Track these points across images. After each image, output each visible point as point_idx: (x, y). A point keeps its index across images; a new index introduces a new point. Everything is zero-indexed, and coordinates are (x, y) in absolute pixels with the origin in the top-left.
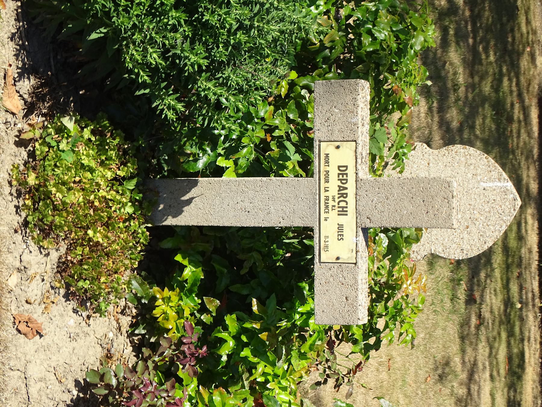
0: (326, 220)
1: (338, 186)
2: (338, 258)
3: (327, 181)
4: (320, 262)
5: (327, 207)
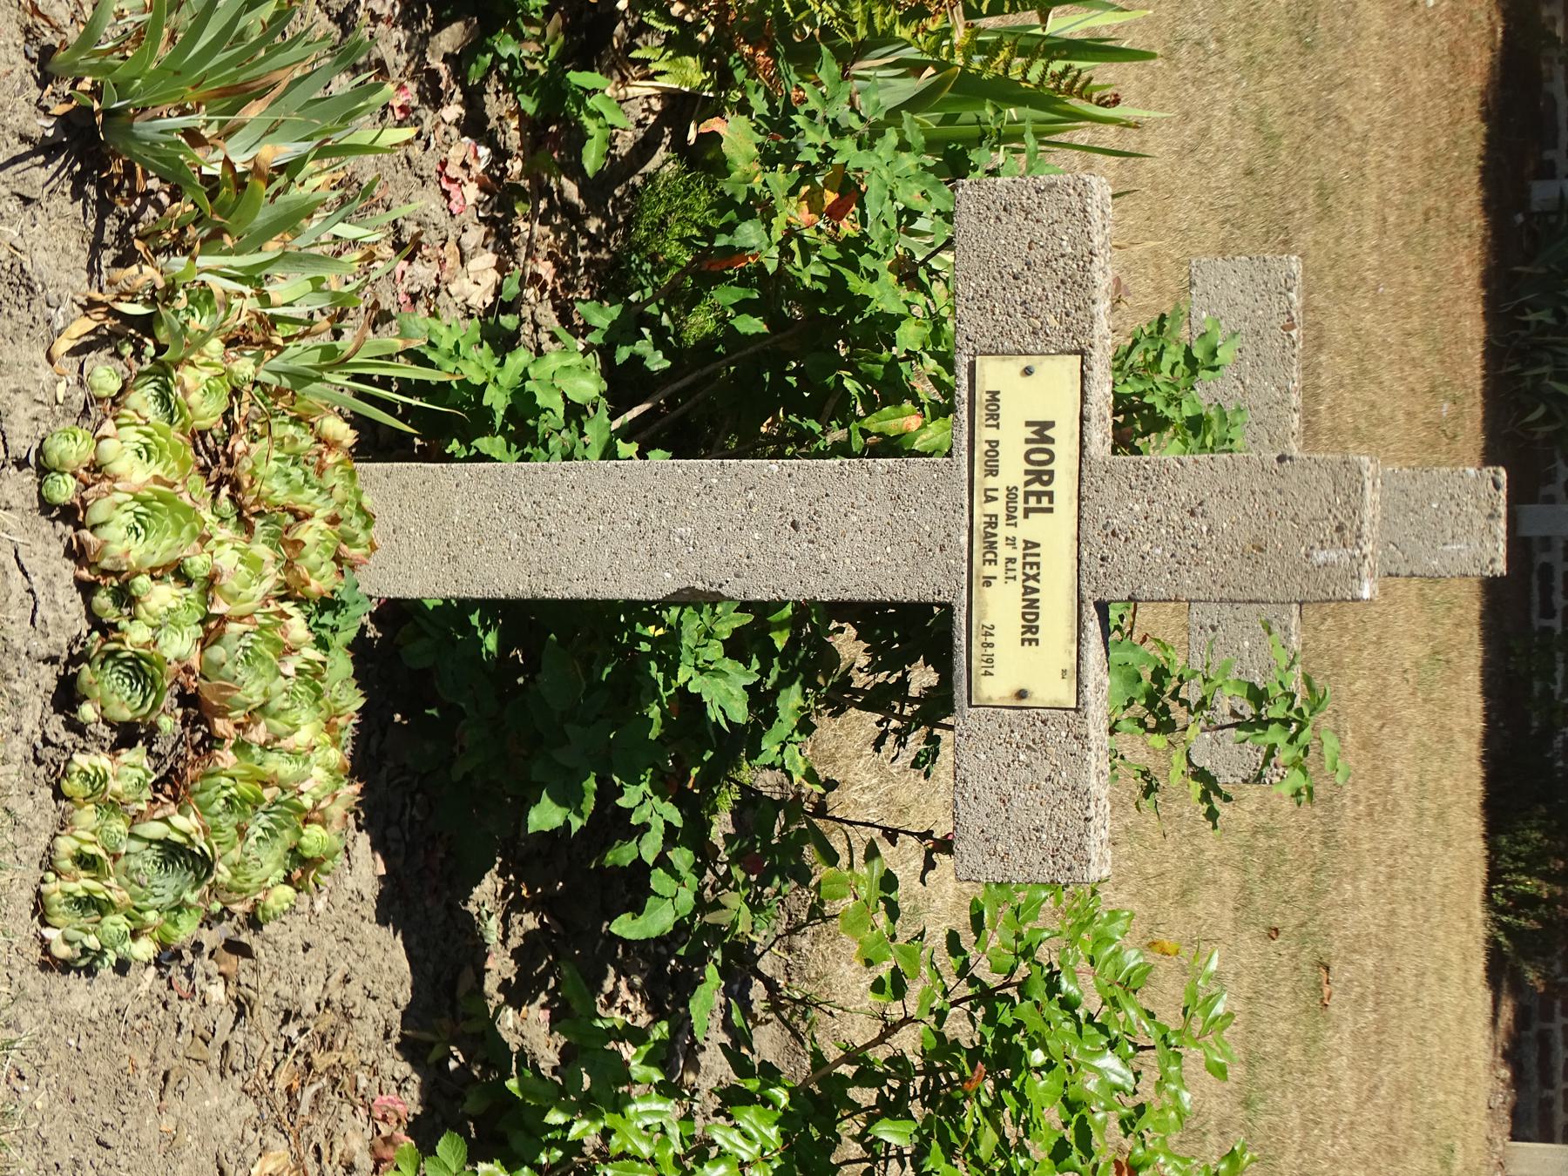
0: (988, 584)
2: (1022, 694)
3: (993, 472)
4: (970, 706)
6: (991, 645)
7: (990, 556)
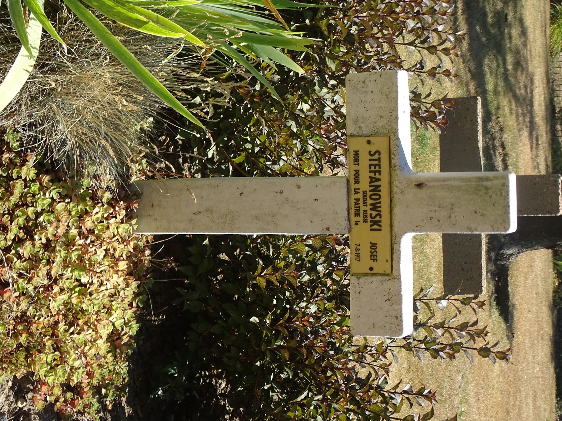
1: (370, 177)
2: (371, 269)
3: (357, 182)
6: (359, 250)
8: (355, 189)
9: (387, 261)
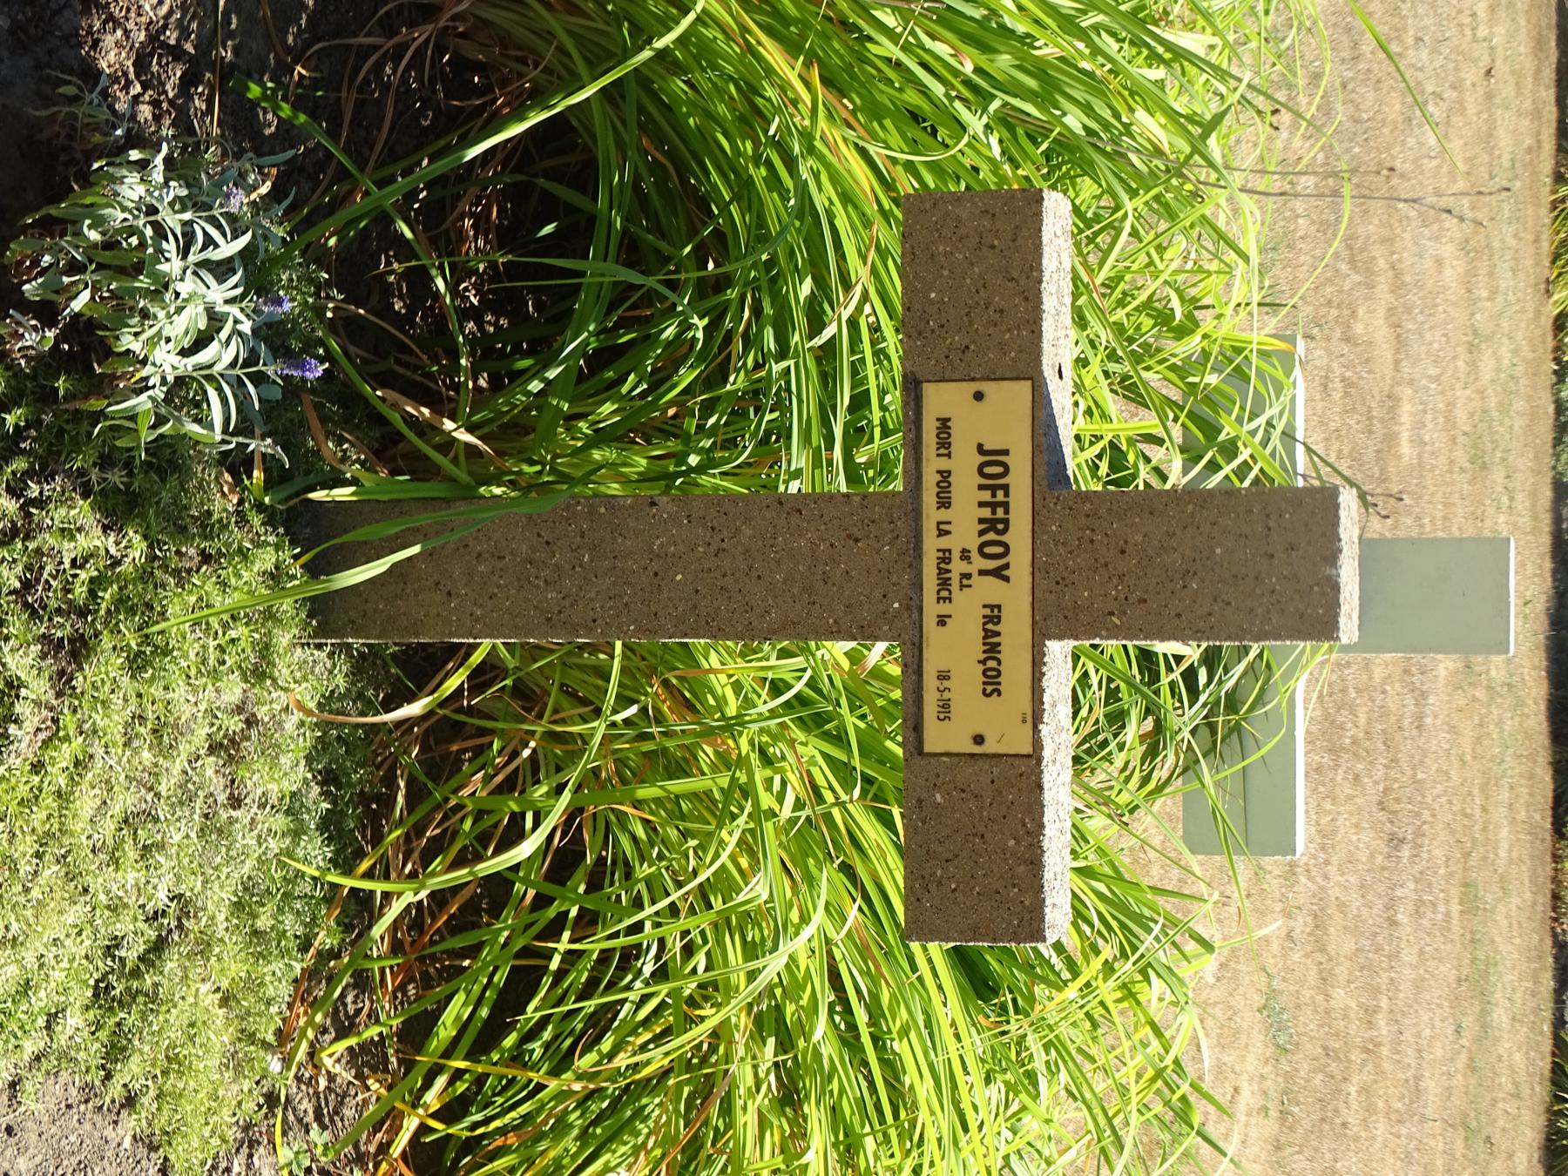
2: (979, 740)
3: (944, 503)
5: (944, 583)
7: (945, 594)
8: (939, 523)
9: (1024, 721)
